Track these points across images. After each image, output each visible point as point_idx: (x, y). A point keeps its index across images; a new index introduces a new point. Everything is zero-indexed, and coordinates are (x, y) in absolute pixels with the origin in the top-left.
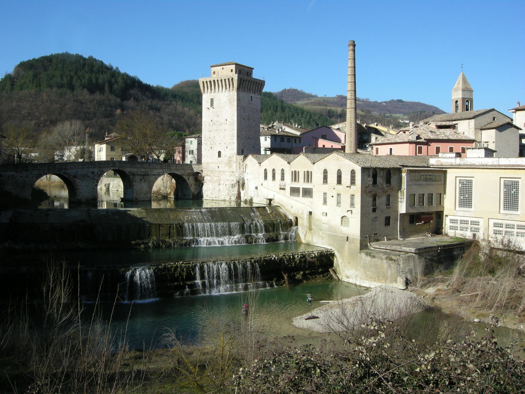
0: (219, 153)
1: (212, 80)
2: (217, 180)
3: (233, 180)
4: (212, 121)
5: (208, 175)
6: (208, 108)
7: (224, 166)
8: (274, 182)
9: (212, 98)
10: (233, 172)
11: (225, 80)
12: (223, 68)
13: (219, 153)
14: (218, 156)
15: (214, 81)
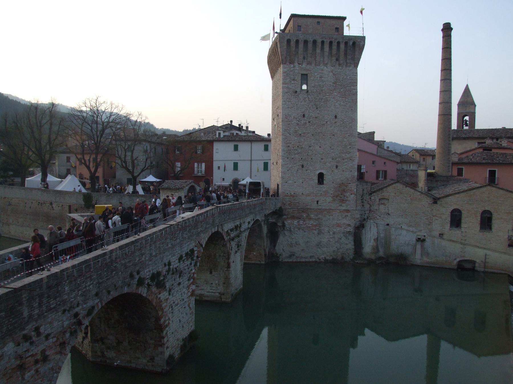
0: (321, 177)
1: (310, 39)
2: (316, 226)
3: (349, 225)
4: (304, 116)
5: (293, 218)
6: (296, 92)
7: (329, 199)
8: (487, 234)
9: (305, 72)
10: (348, 211)
11: (339, 43)
12: (318, 23)
13: (321, 177)
14: (317, 181)
15: (315, 42)
